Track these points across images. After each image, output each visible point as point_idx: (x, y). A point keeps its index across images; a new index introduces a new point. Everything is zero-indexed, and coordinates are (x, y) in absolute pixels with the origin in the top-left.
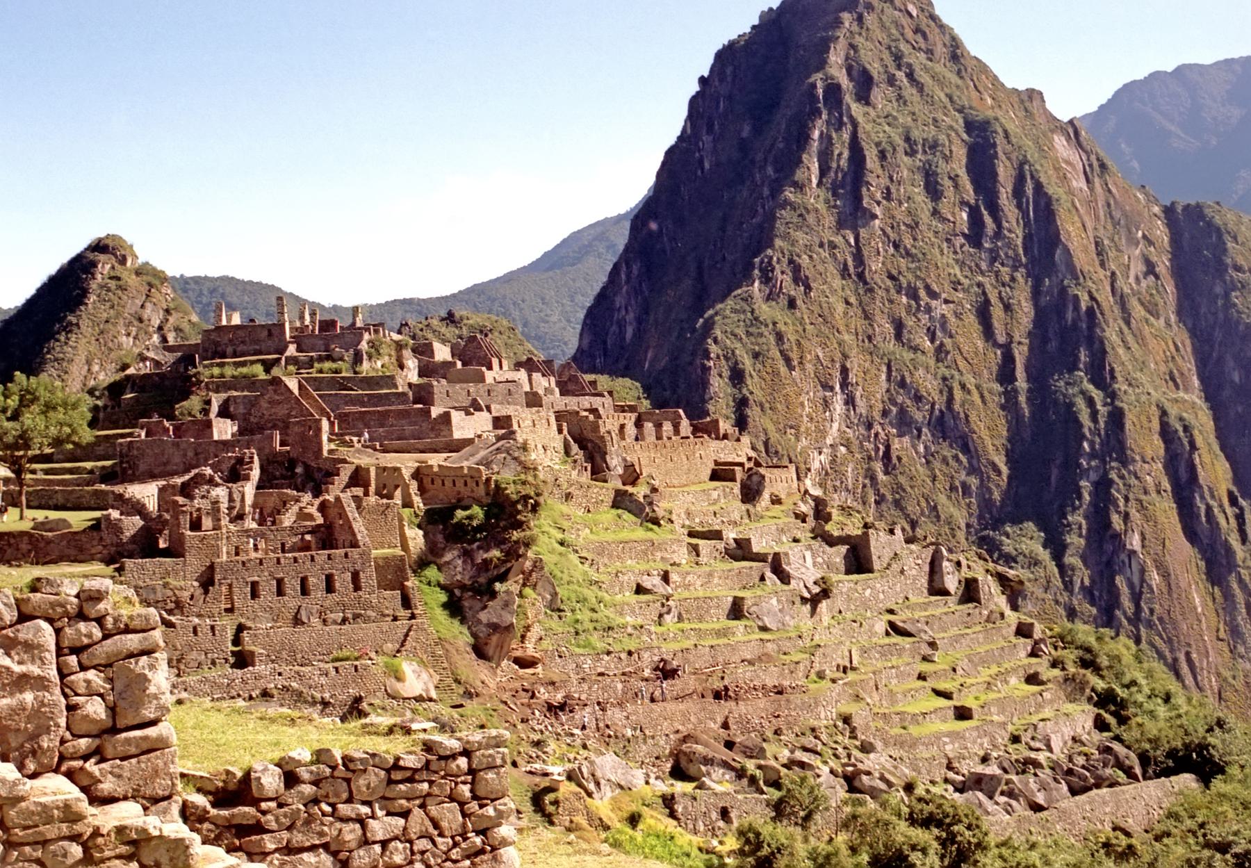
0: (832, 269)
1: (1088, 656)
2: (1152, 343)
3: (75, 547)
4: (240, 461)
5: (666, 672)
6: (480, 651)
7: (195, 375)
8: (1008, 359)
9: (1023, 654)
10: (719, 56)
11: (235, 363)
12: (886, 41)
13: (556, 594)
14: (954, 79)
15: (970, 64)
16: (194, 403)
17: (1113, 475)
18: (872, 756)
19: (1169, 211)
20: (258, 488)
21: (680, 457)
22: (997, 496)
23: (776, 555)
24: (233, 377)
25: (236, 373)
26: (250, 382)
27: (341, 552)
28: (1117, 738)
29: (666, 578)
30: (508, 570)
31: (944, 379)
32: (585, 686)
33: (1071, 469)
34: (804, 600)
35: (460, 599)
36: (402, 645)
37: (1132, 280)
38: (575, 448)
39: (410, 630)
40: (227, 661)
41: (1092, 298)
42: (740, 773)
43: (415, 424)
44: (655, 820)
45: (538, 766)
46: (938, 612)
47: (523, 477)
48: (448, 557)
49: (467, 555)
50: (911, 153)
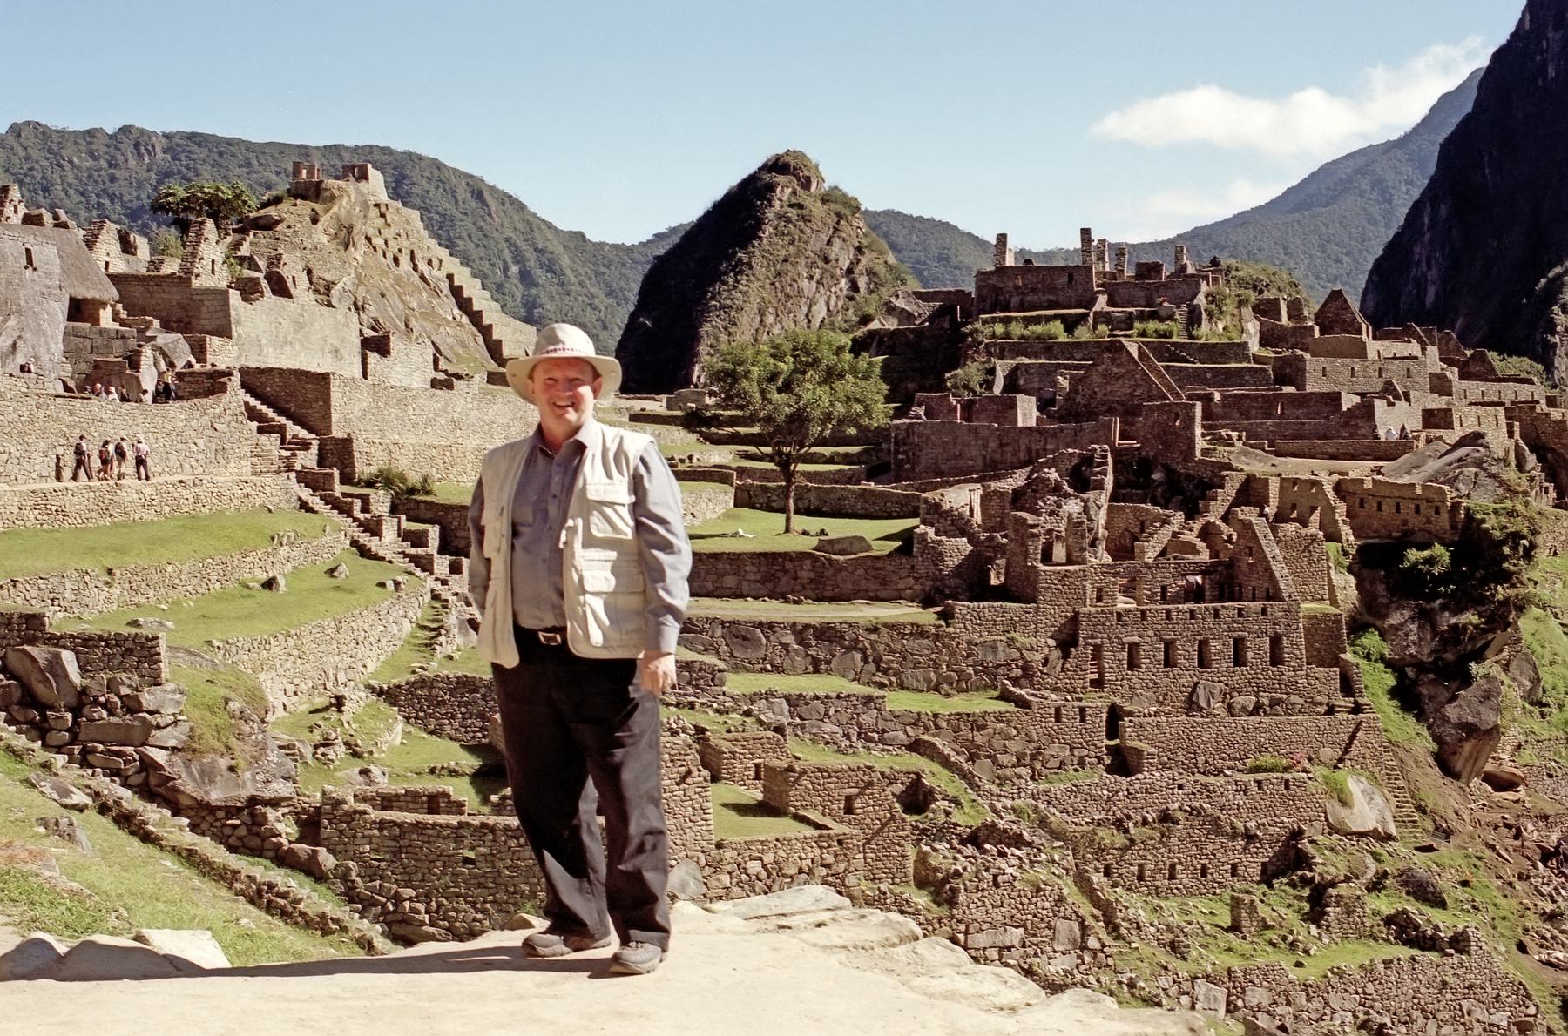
3: (876, 578)
6: (1445, 764)
7: (971, 334)
11: (1024, 318)
13: (1539, 680)
16: (971, 372)
20: (1114, 498)
24: (1023, 337)
25: (1026, 333)
26: (1046, 346)
27: (1258, 605)
30: (1488, 644)
35: (1415, 682)
36: (1346, 752)
38: (1531, 459)
39: (1357, 729)
40: (1100, 759)
43: (1318, 415)
47: (1508, 504)
48: (1395, 619)
49: (1426, 618)
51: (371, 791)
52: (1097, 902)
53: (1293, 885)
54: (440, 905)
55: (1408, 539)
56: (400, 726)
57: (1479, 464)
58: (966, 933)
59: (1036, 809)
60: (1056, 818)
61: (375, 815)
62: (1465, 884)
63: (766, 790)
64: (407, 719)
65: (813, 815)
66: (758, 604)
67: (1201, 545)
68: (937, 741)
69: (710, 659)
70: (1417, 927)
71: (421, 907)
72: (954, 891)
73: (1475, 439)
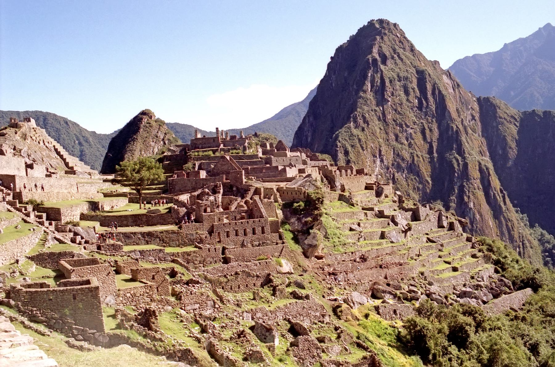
0: (375, 118)
1: (490, 248)
2: (474, 141)
4: (216, 186)
5: (364, 259)
8: (431, 147)
9: (469, 247)
10: (337, 50)
12: (390, 45)
14: (412, 57)
15: (417, 52)
16: (189, 165)
17: (465, 184)
18: (433, 286)
19: (479, 100)
20: (223, 195)
21: (355, 182)
22: (428, 191)
23: (393, 216)
26: (208, 157)
28: (503, 276)
29: (359, 225)
30: (313, 225)
31: (411, 153)
32: (339, 265)
33: (451, 182)
34: (403, 232)
37: (468, 121)
38: (325, 179)
40: (220, 261)
41: (457, 127)
42: (395, 296)
44: (373, 316)
45: (332, 297)
46: (442, 233)
47: (317, 191)
49: (299, 220)
50: (400, 81)
51: (25, 283)
52: (218, 296)
53: (269, 287)
54: (43, 311)
55: (294, 201)
56: (35, 266)
57: (310, 182)
58: (184, 307)
59: (204, 274)
60: (209, 276)
61: (24, 290)
62: (310, 283)
63: (132, 275)
64: (37, 264)
65: (144, 281)
66: (133, 228)
67: (245, 205)
68: (178, 259)
69: (119, 243)
70: (297, 294)
71: (38, 312)
72: (181, 297)
73: (309, 176)
